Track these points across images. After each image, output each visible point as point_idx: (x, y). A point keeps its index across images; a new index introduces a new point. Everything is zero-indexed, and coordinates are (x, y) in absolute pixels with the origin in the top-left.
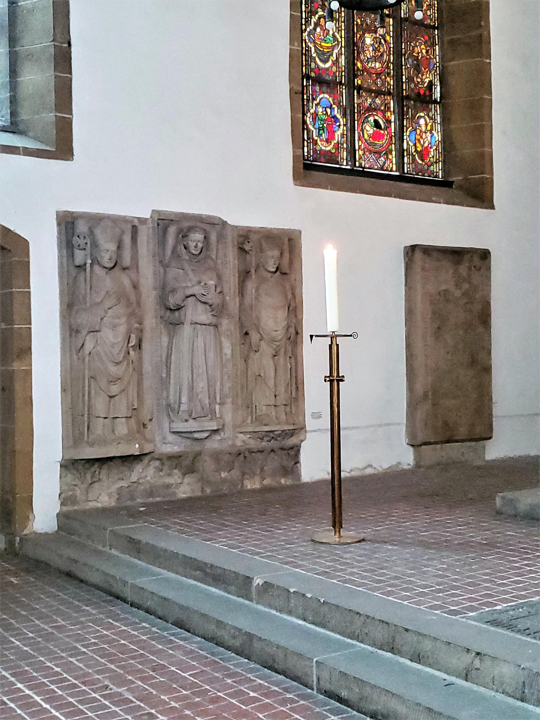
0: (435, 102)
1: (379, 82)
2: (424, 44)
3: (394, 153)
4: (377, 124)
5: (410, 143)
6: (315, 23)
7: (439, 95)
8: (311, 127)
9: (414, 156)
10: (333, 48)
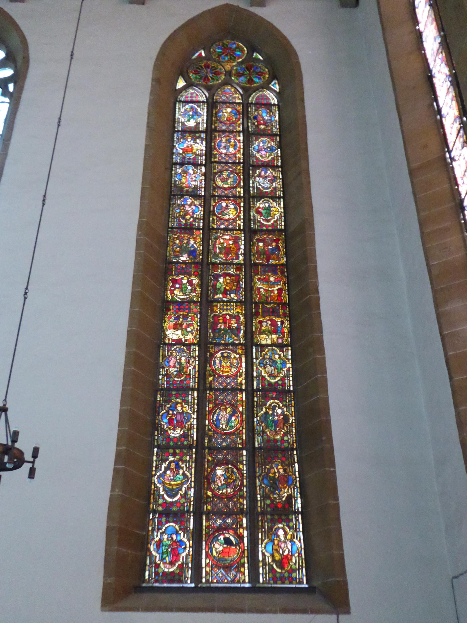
0: (296, 513)
1: (231, 505)
2: (281, 465)
3: (246, 565)
4: (228, 541)
5: (266, 554)
6: (165, 468)
7: (300, 506)
8: (154, 553)
9: (272, 565)
10: (182, 484)
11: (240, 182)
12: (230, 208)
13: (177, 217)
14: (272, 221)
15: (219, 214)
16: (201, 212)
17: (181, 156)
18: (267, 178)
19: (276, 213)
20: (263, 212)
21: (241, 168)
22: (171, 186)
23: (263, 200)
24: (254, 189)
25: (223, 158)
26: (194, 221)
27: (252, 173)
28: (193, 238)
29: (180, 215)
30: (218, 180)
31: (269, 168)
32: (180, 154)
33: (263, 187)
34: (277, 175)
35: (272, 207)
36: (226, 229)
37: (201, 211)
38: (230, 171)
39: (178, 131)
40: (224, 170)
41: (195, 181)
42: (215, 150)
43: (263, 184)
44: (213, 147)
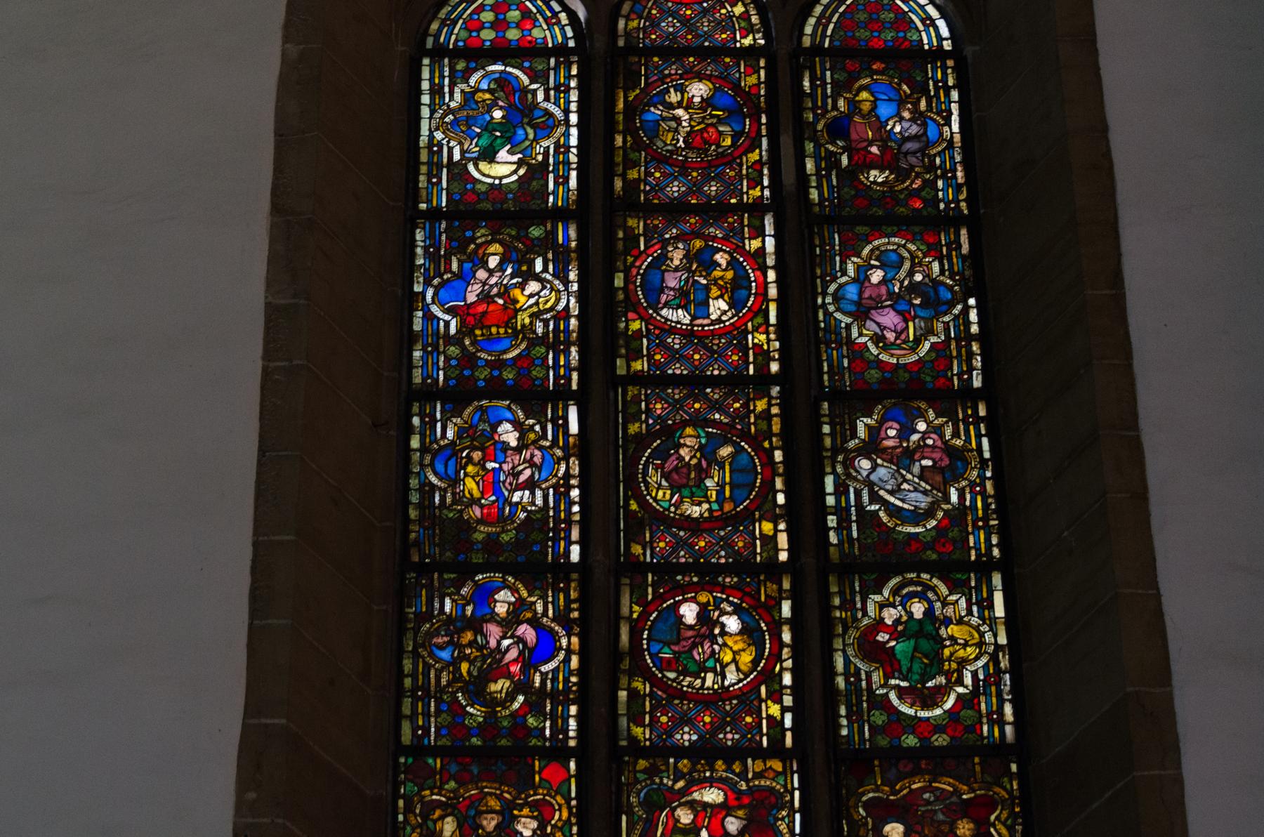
11: (770, 489)
12: (724, 633)
13: (440, 689)
14: (950, 703)
15: (665, 665)
16: (567, 660)
17: (454, 351)
18: (913, 461)
19: (971, 652)
20: (902, 648)
21: (775, 410)
22: (407, 520)
23: (894, 582)
24: (843, 525)
25: (674, 356)
26: (534, 706)
27: (833, 434)
28: (534, 805)
29: (457, 677)
30: (654, 477)
31: (923, 405)
32: (449, 340)
33: (894, 512)
34: (968, 440)
35: (947, 622)
36: (706, 751)
37: (569, 652)
38: (715, 424)
39: (435, 214)
40: (685, 424)
41: (531, 485)
42: (631, 315)
43: (891, 493)
44: (621, 296)
